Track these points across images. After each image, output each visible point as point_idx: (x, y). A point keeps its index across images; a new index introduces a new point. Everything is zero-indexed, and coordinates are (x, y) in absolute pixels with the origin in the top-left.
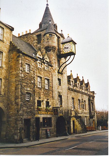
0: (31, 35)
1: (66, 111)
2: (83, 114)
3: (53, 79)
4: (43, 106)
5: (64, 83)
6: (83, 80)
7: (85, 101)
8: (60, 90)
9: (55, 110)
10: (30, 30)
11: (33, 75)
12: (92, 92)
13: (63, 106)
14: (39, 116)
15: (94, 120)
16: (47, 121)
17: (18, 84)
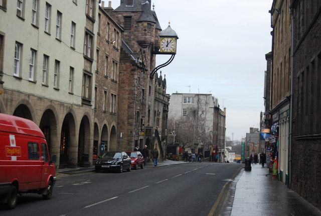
10: (110, 2)
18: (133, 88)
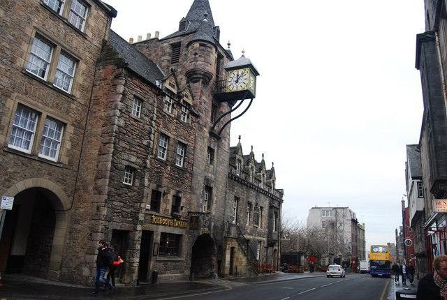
0: (158, 43)
1: (219, 224)
2: (255, 236)
3: (198, 147)
4: (166, 205)
5: (221, 160)
6: (263, 161)
7: (262, 208)
8: (210, 175)
9: (194, 220)
10: (157, 33)
11: (147, 127)
12: (277, 191)
13: (213, 213)
14: (153, 227)
15: (275, 250)
16: (171, 244)
17: (107, 141)
18: (111, 113)
